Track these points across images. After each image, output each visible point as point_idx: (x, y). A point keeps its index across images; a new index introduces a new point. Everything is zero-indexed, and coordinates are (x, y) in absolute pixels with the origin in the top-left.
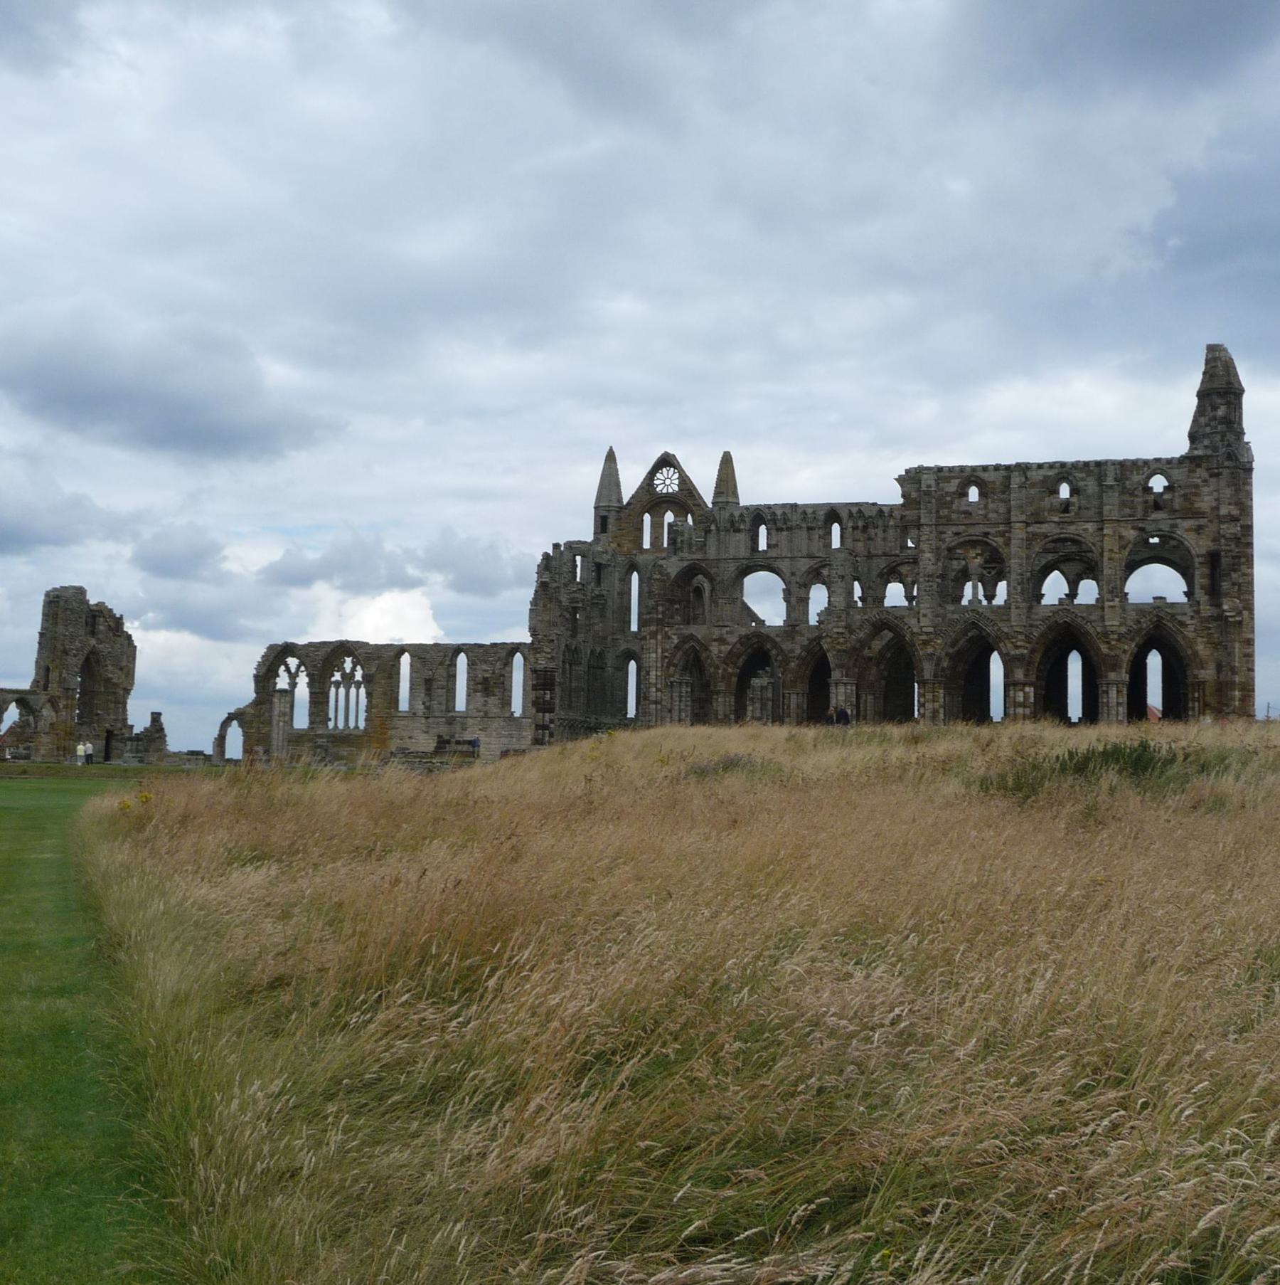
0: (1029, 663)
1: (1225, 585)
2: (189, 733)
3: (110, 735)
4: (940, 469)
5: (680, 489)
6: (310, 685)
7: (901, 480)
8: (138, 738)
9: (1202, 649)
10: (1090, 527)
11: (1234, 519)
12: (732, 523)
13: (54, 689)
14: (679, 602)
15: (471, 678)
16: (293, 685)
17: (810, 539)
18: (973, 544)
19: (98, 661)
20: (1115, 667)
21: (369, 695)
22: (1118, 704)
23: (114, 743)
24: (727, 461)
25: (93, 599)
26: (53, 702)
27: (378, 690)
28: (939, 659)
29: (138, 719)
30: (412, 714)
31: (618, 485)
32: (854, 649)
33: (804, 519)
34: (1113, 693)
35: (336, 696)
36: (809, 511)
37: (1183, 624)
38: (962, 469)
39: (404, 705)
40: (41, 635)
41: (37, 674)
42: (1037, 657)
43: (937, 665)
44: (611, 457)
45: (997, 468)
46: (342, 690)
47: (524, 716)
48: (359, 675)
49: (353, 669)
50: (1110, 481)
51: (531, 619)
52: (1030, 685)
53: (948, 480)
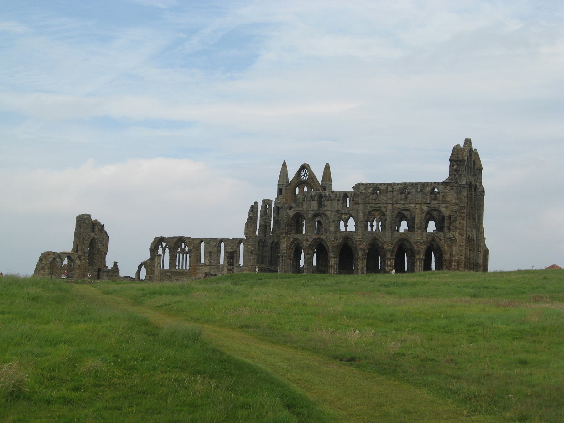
0: (393, 252)
1: (451, 227)
2: (127, 270)
3: (99, 270)
4: (366, 184)
5: (309, 178)
6: (169, 253)
7: (354, 187)
8: (109, 271)
9: (446, 248)
10: (413, 205)
11: (457, 204)
12: (312, 197)
13: (80, 253)
14: (294, 226)
15: (226, 252)
16: (164, 253)
17: (338, 204)
18: (377, 210)
19: (95, 242)
20: (419, 253)
21: (190, 257)
22: (420, 266)
23: (101, 273)
24: (327, 167)
25: (93, 218)
26: (79, 257)
27: (193, 255)
28: (364, 250)
29: (109, 265)
30: (205, 264)
31: (287, 176)
32: (337, 246)
33: (336, 197)
34: (418, 263)
35: (179, 257)
36: (338, 194)
37: (440, 240)
38: (373, 184)
39: (202, 261)
40: (75, 233)
41: (74, 246)
42: (396, 250)
43: (364, 252)
44: (284, 165)
45: (385, 184)
46: (181, 255)
47: (243, 266)
48: (187, 250)
49: (185, 247)
50: (419, 190)
51: (245, 230)
52: (393, 259)
53: (369, 188)
